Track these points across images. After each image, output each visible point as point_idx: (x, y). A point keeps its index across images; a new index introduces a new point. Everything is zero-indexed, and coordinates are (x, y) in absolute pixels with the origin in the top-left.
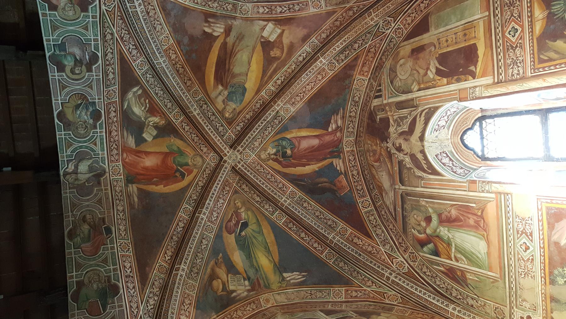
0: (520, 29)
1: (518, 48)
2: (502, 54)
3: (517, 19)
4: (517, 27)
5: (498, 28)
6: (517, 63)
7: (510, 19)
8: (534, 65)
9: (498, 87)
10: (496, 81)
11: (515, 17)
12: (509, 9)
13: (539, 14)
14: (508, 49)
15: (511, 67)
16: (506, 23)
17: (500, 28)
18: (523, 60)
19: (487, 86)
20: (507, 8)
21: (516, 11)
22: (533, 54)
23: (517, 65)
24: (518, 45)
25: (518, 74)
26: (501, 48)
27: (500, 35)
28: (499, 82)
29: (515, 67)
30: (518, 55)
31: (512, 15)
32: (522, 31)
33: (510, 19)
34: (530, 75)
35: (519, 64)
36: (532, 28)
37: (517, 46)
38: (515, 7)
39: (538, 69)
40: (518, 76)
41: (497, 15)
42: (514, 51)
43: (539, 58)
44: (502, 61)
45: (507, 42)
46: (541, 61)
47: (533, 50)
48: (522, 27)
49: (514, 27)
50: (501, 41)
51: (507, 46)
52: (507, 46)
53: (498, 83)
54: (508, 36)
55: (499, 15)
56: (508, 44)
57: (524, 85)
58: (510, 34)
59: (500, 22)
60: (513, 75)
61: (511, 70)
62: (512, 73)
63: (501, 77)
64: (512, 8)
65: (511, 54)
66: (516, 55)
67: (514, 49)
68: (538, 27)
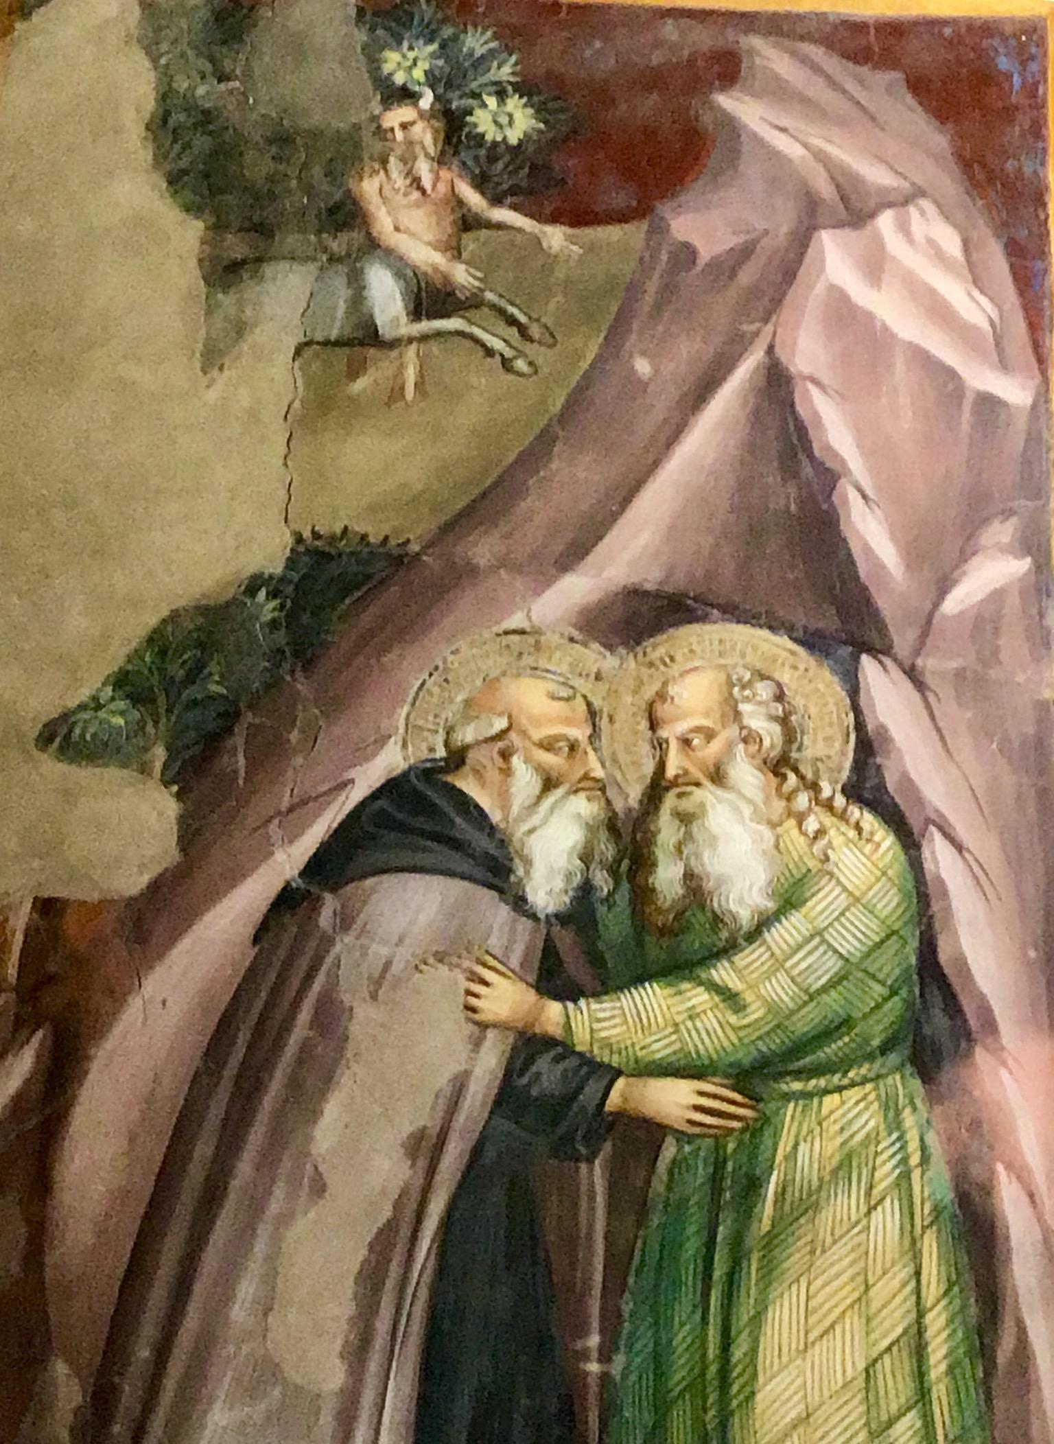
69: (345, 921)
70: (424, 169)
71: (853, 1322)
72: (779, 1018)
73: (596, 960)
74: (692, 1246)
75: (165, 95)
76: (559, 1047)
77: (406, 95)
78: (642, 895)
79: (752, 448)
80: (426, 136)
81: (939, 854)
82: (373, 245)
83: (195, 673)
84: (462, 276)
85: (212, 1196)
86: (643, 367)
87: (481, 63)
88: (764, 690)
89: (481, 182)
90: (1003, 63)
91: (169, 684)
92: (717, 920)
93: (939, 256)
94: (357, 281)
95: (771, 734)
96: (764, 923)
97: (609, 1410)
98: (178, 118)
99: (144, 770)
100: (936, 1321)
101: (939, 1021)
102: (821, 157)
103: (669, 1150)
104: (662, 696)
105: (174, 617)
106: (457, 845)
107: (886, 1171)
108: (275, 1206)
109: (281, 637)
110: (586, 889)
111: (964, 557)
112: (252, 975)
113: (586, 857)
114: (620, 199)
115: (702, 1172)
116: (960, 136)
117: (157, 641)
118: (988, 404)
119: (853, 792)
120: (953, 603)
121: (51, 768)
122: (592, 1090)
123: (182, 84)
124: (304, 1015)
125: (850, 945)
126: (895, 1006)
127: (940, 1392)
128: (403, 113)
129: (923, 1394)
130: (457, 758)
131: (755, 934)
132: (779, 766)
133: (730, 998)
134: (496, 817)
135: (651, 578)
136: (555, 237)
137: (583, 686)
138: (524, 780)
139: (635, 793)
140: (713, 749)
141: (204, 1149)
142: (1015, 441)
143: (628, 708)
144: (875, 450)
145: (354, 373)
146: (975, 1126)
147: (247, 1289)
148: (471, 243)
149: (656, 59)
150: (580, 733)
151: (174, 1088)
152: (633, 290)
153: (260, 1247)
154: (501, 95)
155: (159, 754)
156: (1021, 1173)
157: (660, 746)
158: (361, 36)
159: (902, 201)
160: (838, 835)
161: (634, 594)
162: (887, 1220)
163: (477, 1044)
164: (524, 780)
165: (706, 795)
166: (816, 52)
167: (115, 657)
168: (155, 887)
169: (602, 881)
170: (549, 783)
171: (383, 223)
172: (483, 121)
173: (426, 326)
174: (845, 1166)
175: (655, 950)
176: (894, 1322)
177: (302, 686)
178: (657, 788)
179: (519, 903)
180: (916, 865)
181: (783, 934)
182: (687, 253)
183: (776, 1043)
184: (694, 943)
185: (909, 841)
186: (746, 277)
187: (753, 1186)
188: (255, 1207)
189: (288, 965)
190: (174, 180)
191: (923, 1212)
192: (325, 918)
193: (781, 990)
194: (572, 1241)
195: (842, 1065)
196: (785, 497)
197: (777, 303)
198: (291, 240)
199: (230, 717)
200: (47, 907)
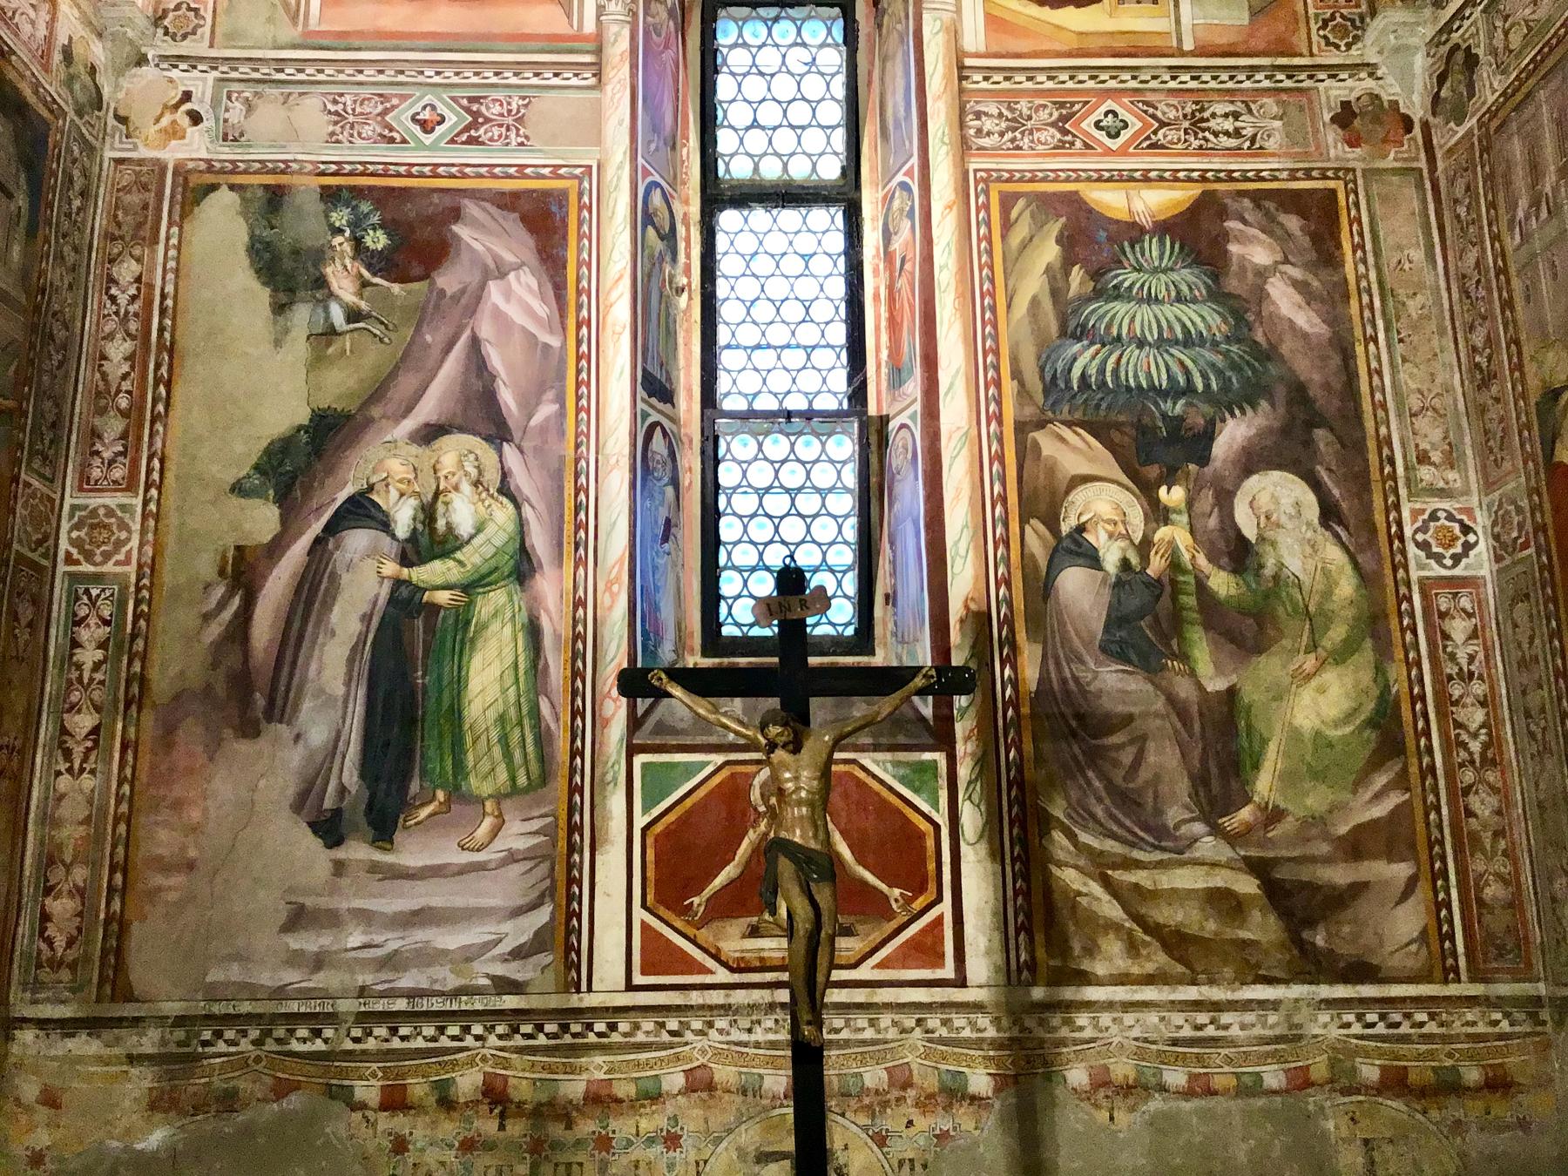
0: (1114, 144)
1: (1058, 136)
2: (1050, 85)
3: (1149, 138)
4: (1125, 135)
5: (1134, 78)
6: (1014, 130)
7: (1153, 116)
8: (999, 180)
9: (948, 67)
10: (968, 62)
11: (1155, 133)
12: (1185, 116)
13: (1152, 203)
14: (1062, 105)
15: (1006, 113)
16: (1144, 103)
17: (1133, 84)
18: (1020, 148)
19: (955, 33)
20: (1188, 110)
21: (1172, 135)
22: (1031, 180)
23: (1008, 129)
24: (1069, 138)
25: (979, 131)
26: (1070, 85)
27: (1112, 84)
28: (962, 72)
29: (1004, 125)
30: (1036, 135)
31: (1163, 124)
32: (1109, 152)
33: (1153, 116)
34: (972, 167)
35: (1009, 135)
36: (1109, 180)
37: (1066, 132)
38: (1186, 133)
39: (987, 192)
40: (972, 132)
41: (1174, 78)
42: (1053, 124)
43: (1017, 196)
44: (1029, 85)
45: (1086, 103)
46: (1007, 201)
47: (1044, 180)
48: (1123, 152)
49: (1126, 126)
50: (1091, 84)
51: (1073, 104)
52: (1073, 104)
53: (961, 67)
54: (1103, 109)
55: (1173, 84)
56: (1077, 107)
57: (945, 148)
58: (1106, 114)
59: (1154, 84)
60: (978, 115)
61: (995, 112)
62: (986, 114)
63: (978, 77)
64: (1186, 124)
65: (1043, 115)
66: (1038, 130)
67: (1060, 124)
68: (1110, 200)
69: (337, 548)
70: (348, 262)
71: (497, 662)
72: (477, 568)
73: (418, 553)
74: (449, 644)
75: (252, 236)
76: (408, 583)
77: (340, 231)
78: (433, 530)
79: (467, 369)
80: (347, 248)
81: (527, 511)
82: (331, 295)
83: (281, 464)
84: (364, 305)
85: (300, 638)
86: (428, 338)
87: (366, 216)
88: (472, 457)
89: (369, 267)
90: (554, 209)
91: (273, 468)
92: (457, 538)
93: (531, 290)
94: (326, 310)
95: (474, 472)
96: (472, 537)
97: (425, 693)
98: (258, 245)
99: (267, 499)
100: (521, 659)
101: (526, 566)
102: (489, 249)
103: (442, 613)
104: (437, 462)
105: (272, 443)
106: (372, 518)
107: (508, 615)
108: (320, 640)
109: (310, 448)
110: (415, 529)
111: (538, 404)
112: (308, 566)
113: (414, 519)
114: (417, 270)
115: (451, 621)
116: (537, 241)
117: (268, 452)
118: (546, 346)
119: (501, 491)
120: (533, 423)
121: (235, 501)
122: (418, 595)
123: (257, 232)
124: (325, 580)
125: (498, 543)
126: (512, 562)
127: (522, 680)
128: (339, 239)
129: (517, 679)
130: (371, 488)
131: (468, 542)
132: (477, 484)
133: (460, 563)
134: (384, 507)
135: (433, 419)
136: (396, 288)
137: (412, 460)
138: (394, 494)
139: (430, 497)
140: (454, 480)
141: (296, 625)
142: (554, 362)
143: (426, 467)
144: (510, 367)
145: (329, 345)
146: (535, 599)
147: (313, 667)
148: (368, 291)
149: (430, 210)
150: (411, 476)
151: (286, 604)
152: (424, 310)
153: (317, 652)
154: (374, 230)
155: (271, 492)
156: (547, 611)
157: (438, 479)
158: (322, 207)
159: (517, 267)
160: (495, 506)
161: (427, 425)
162: (508, 630)
163: (381, 583)
164: (394, 494)
165: (453, 496)
166: (487, 205)
167: (254, 459)
168: (273, 539)
169: (420, 527)
170: (402, 495)
171: (334, 286)
172: (368, 241)
173: (352, 326)
174: (495, 615)
175: (437, 550)
176: (509, 660)
177: (319, 466)
178: (437, 494)
179: (393, 536)
180: (520, 514)
181: (476, 541)
182: (442, 292)
183: (476, 576)
184: (448, 546)
185: (518, 507)
186: (463, 301)
187: (468, 623)
188: (314, 642)
189: (320, 561)
190: (258, 271)
191: (519, 627)
192: (331, 546)
193: (477, 559)
194: (412, 643)
195: (496, 582)
196: (478, 385)
197: (474, 312)
198: (301, 294)
199: (294, 478)
200: (238, 548)
